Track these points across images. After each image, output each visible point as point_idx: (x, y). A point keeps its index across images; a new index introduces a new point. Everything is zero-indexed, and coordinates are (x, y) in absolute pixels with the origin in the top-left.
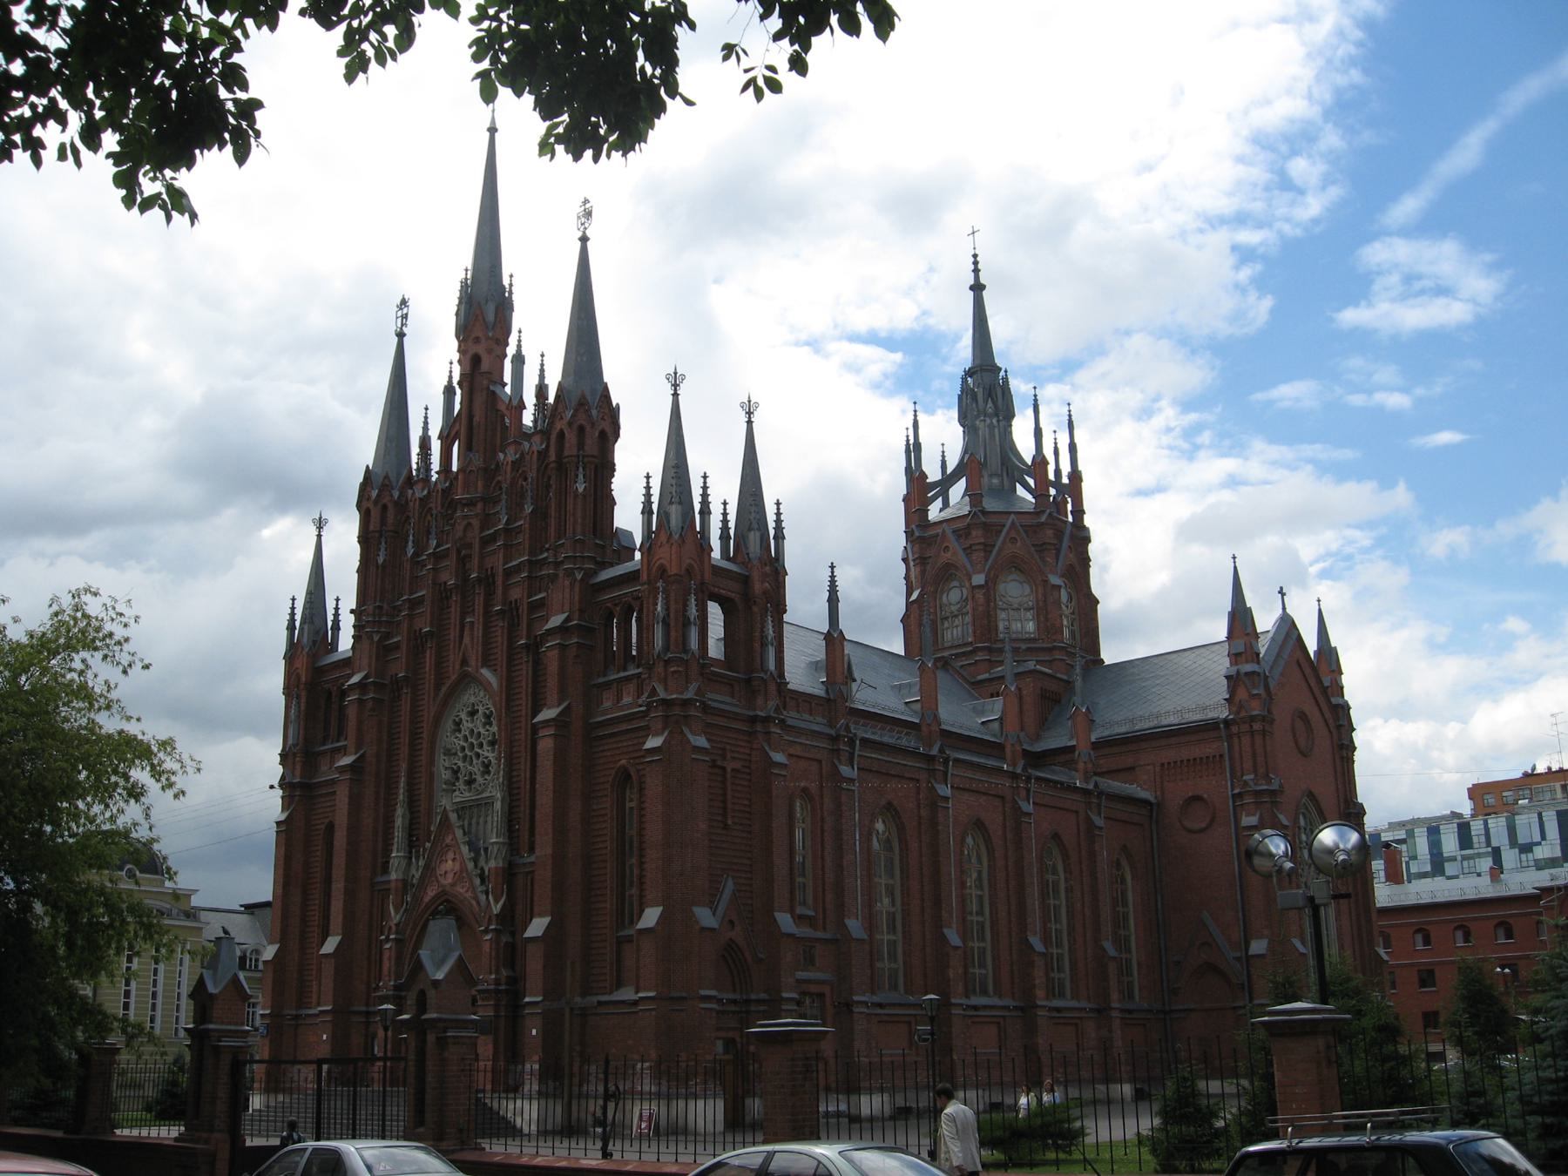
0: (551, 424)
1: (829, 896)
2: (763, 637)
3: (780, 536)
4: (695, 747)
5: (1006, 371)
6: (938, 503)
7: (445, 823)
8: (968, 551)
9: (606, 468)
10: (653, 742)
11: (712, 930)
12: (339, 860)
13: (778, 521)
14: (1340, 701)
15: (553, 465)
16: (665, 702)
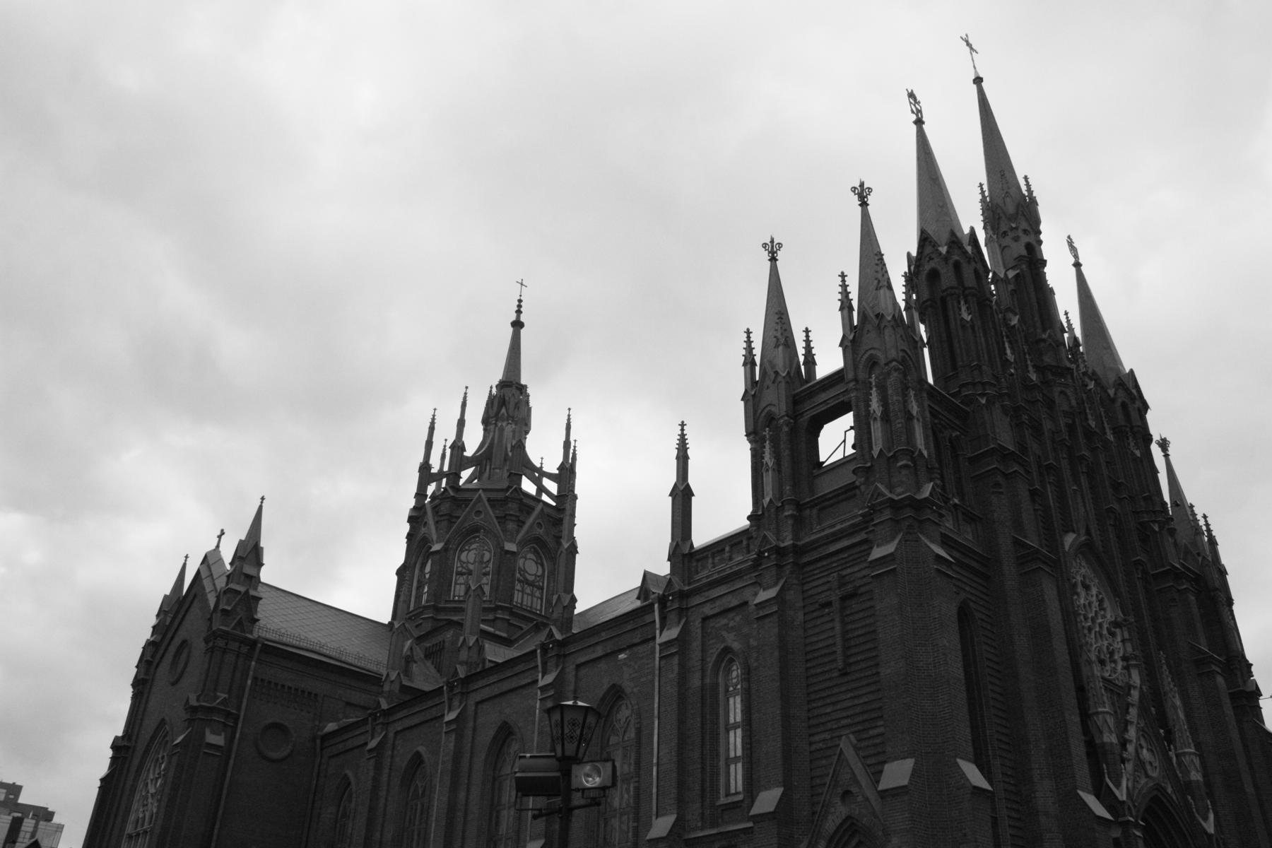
8: (502, 519)
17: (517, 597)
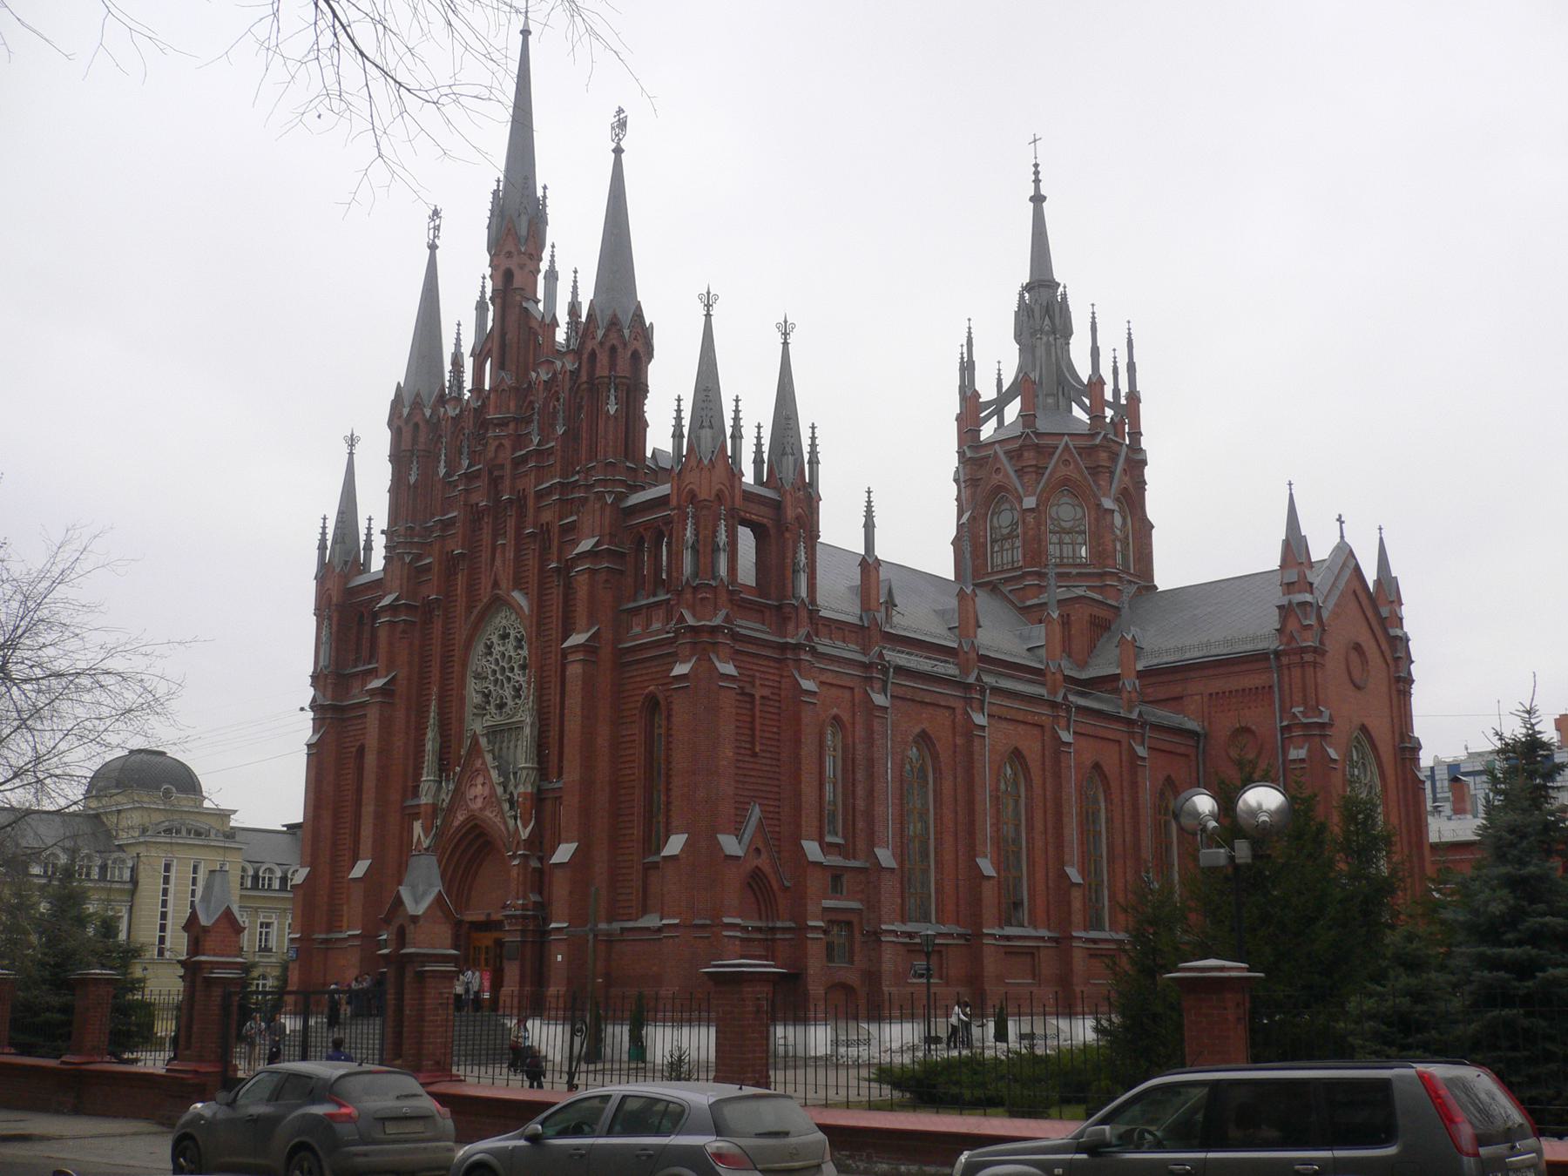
0: (582, 344)
1: (860, 825)
2: (795, 564)
3: (814, 461)
4: (722, 674)
5: (1065, 287)
6: (993, 422)
7: (475, 748)
8: (1020, 472)
9: (636, 390)
10: (681, 669)
11: (738, 858)
12: (370, 782)
13: (813, 445)
14: (1399, 633)
15: (585, 386)
16: (692, 628)
17: (1053, 550)
